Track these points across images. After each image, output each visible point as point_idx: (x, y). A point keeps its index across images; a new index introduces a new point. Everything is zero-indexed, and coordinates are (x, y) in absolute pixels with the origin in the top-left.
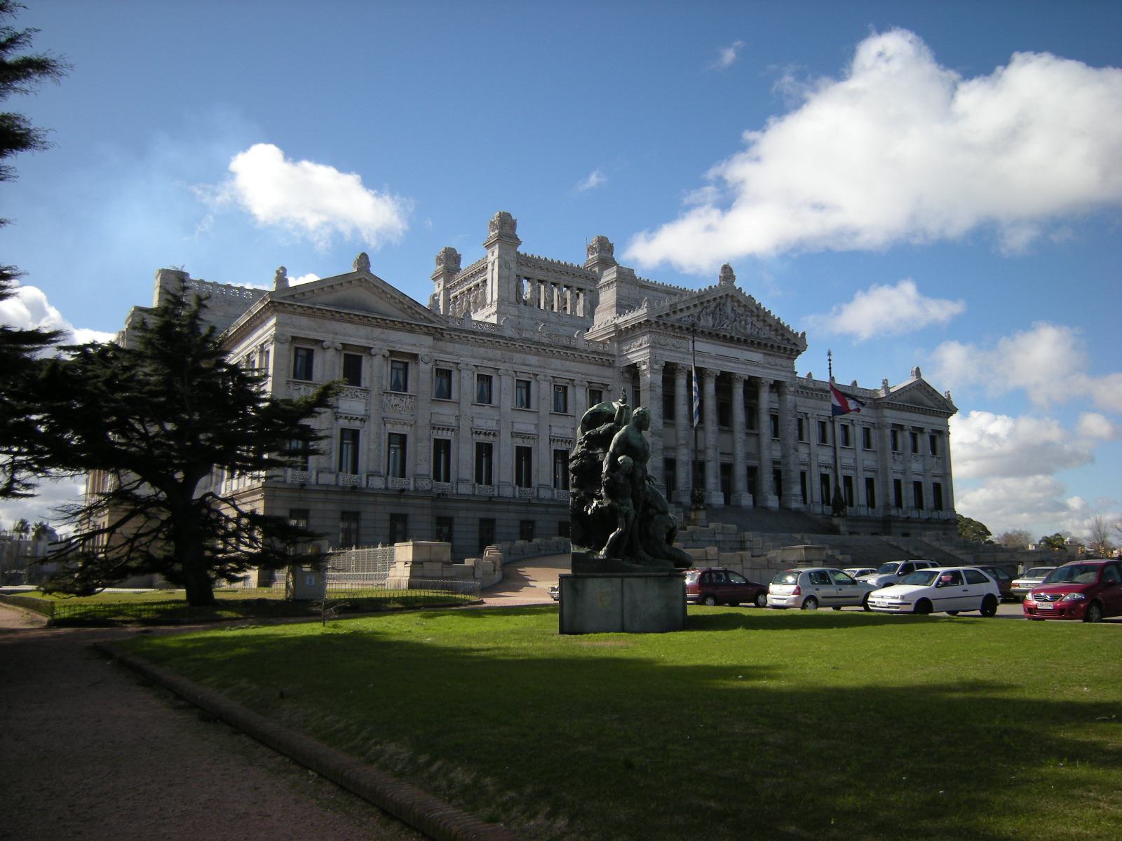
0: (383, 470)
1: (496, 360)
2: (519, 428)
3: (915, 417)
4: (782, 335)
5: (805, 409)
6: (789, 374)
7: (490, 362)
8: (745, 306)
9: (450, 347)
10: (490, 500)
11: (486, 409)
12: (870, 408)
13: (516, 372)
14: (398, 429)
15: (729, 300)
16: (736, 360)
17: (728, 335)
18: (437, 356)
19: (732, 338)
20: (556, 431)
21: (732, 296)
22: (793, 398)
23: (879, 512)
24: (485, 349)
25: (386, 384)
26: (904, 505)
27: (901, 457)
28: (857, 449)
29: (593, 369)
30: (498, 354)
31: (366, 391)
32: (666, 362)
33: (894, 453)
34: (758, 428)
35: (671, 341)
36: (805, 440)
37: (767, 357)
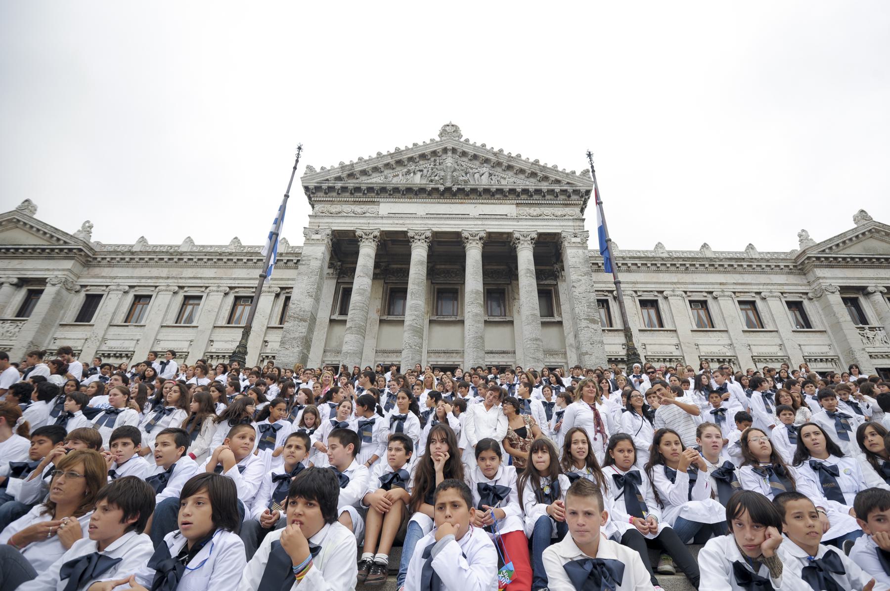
4: (546, 178)
5: (658, 286)
6: (571, 223)
7: (149, 281)
8: (475, 157)
9: (106, 271)
11: (131, 331)
12: (789, 273)
13: (181, 287)
15: (450, 154)
16: (464, 217)
17: (442, 188)
18: (84, 281)
19: (448, 190)
21: (454, 150)
22: (580, 251)
24: (149, 269)
27: (881, 334)
28: (780, 330)
30: (164, 272)
32: (333, 231)
33: (863, 329)
34: (560, 314)
35: (347, 208)
36: (667, 327)
37: (527, 209)
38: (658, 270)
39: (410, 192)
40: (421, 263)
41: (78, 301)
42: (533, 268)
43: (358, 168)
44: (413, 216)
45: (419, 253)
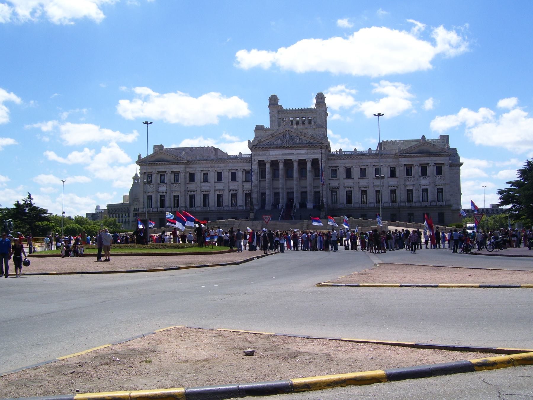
0: (172, 205)
1: (208, 167)
2: (217, 188)
3: (422, 159)
9: (193, 166)
10: (206, 212)
11: (206, 183)
14: (176, 194)
16: (293, 154)
18: (188, 169)
20: (231, 187)
23: (396, 205)
25: (173, 181)
26: (414, 200)
27: (413, 179)
29: (245, 164)
30: (209, 165)
31: (167, 184)
35: (261, 153)
36: (352, 177)
38: (352, 159)
39: (277, 147)
40: (282, 169)
41: (188, 176)
42: (311, 170)
43: (262, 140)
44: (279, 155)
45: (281, 166)
